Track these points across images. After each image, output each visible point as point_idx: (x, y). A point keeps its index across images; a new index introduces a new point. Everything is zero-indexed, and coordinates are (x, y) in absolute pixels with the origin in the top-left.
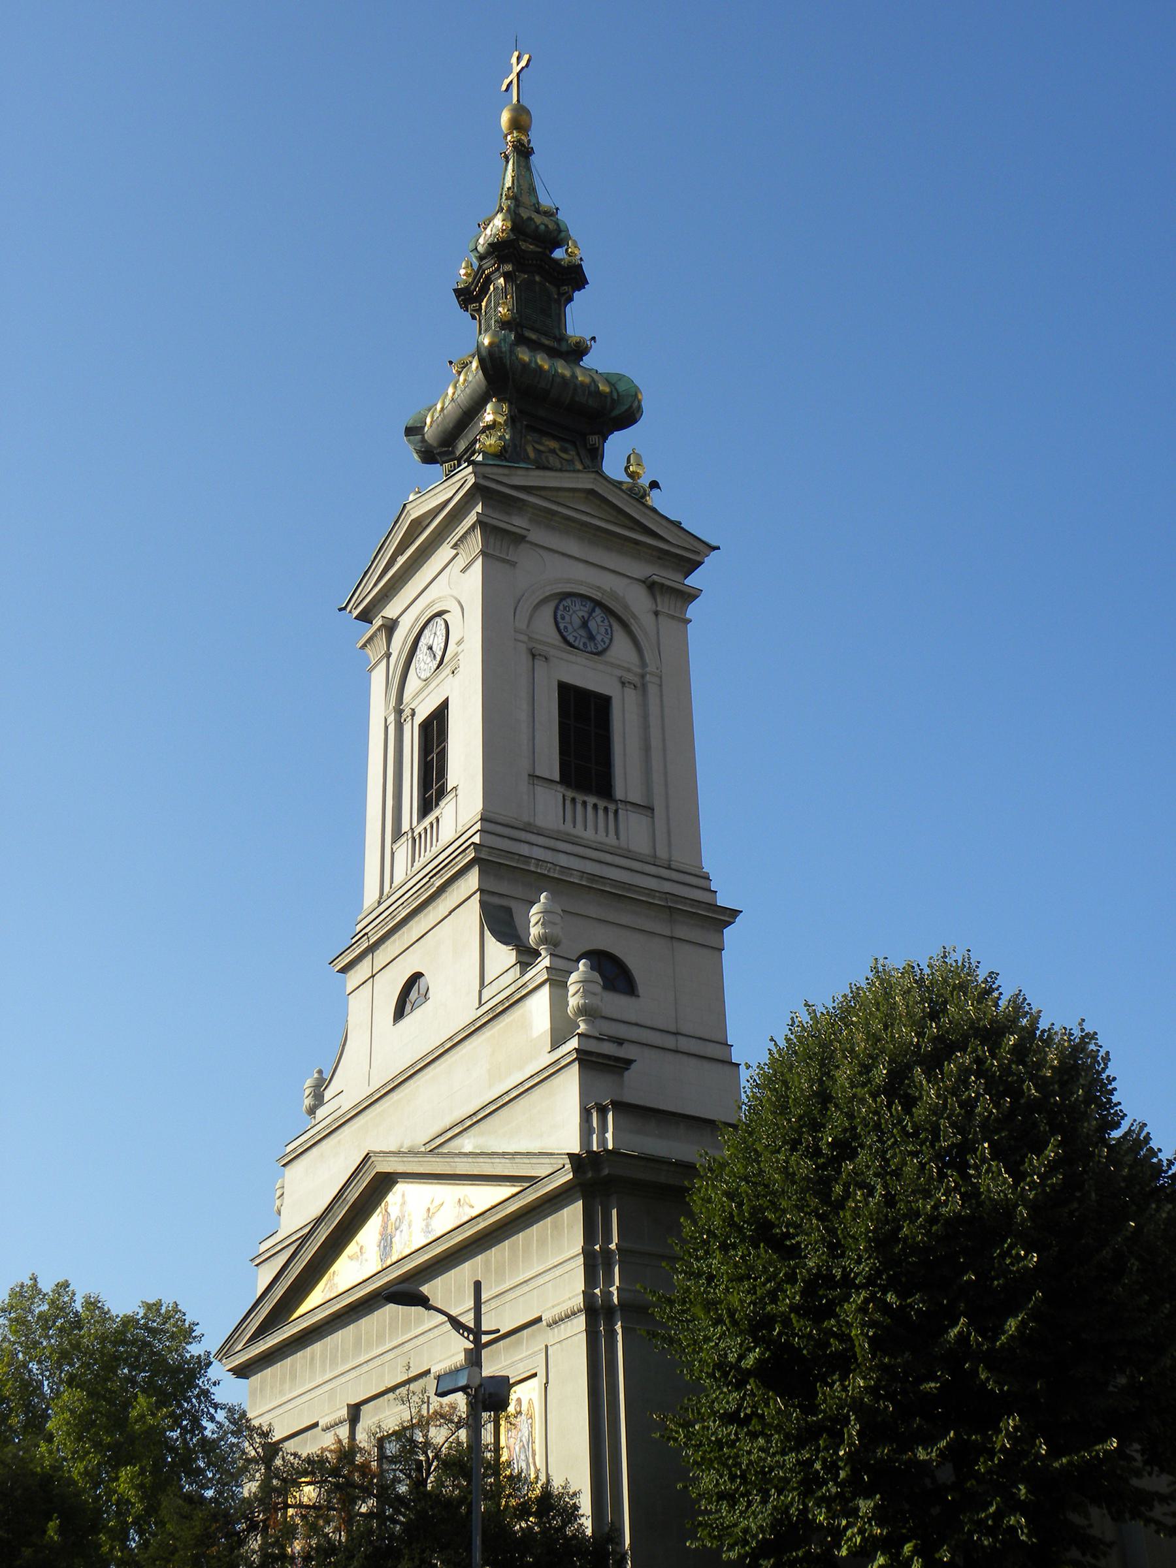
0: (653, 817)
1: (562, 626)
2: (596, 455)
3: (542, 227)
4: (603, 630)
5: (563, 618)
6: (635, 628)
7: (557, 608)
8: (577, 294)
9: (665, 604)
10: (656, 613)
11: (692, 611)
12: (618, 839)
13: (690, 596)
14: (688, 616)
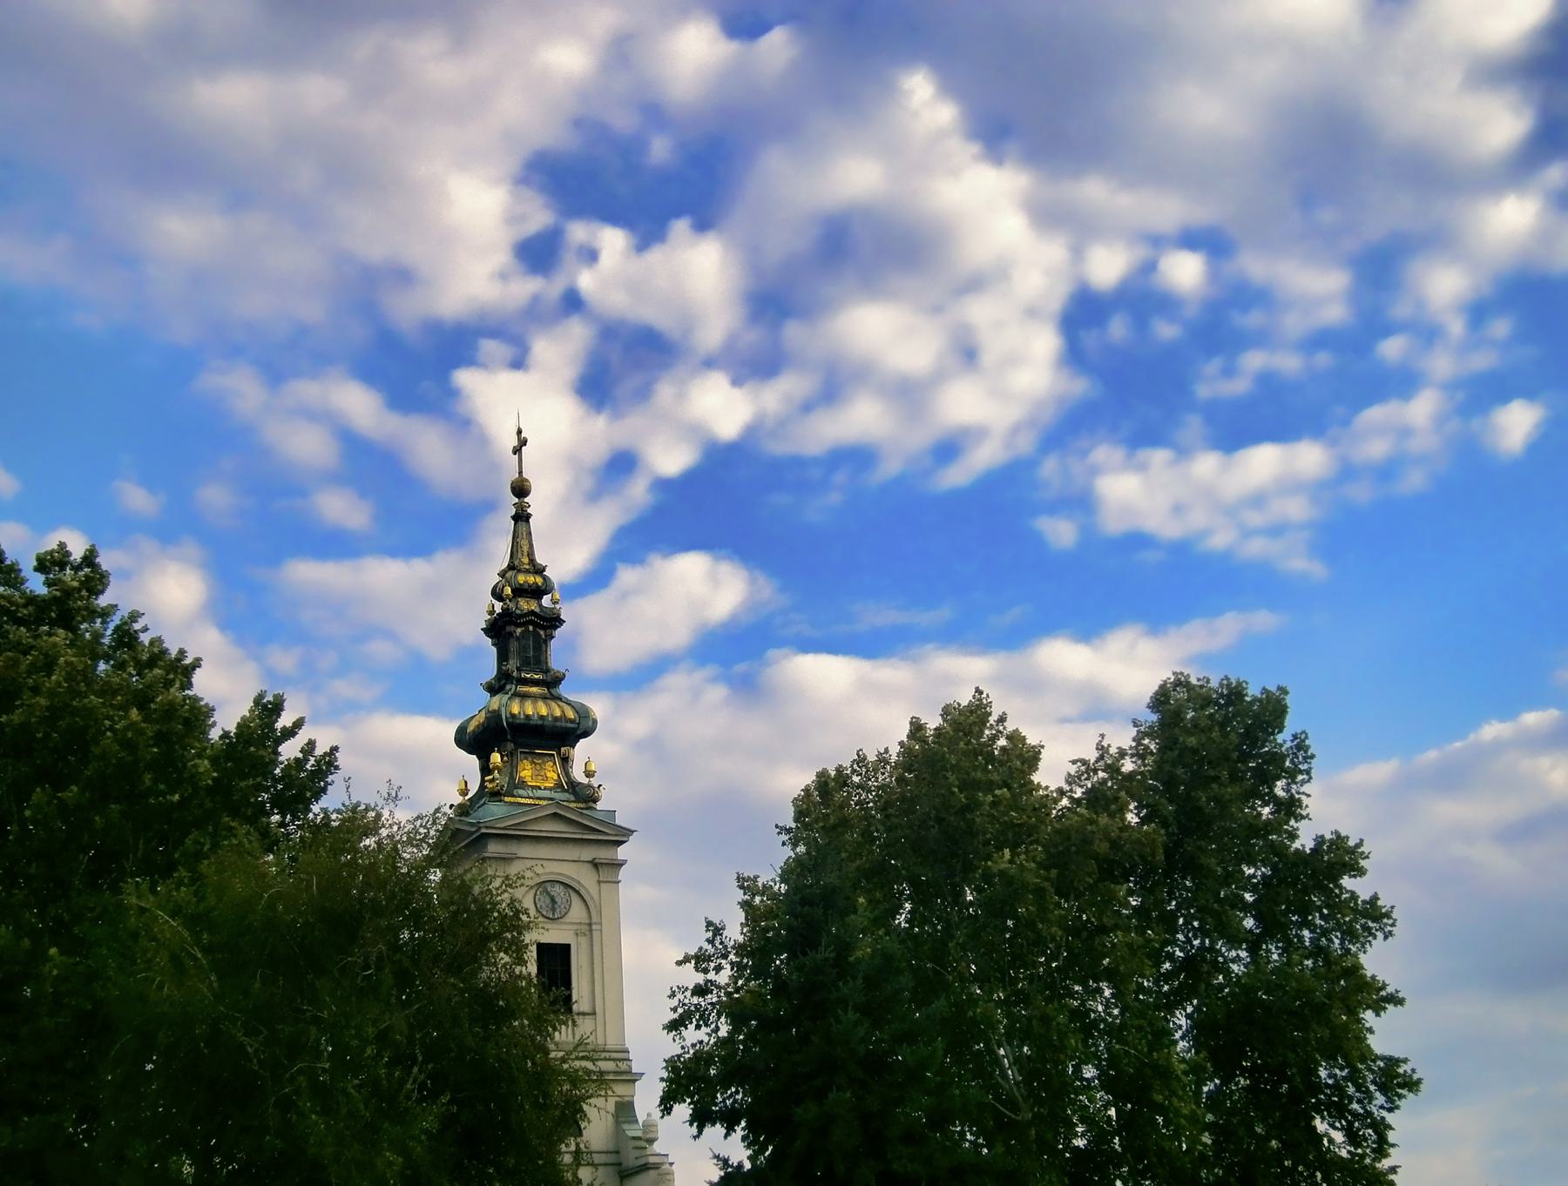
0: (595, 1019)
1: (538, 906)
2: (565, 760)
3: (535, 585)
4: (564, 900)
5: (539, 900)
6: (583, 892)
7: (535, 895)
8: (558, 633)
9: (605, 874)
10: (599, 882)
11: (623, 873)
12: (574, 1038)
13: (618, 865)
14: (619, 878)
